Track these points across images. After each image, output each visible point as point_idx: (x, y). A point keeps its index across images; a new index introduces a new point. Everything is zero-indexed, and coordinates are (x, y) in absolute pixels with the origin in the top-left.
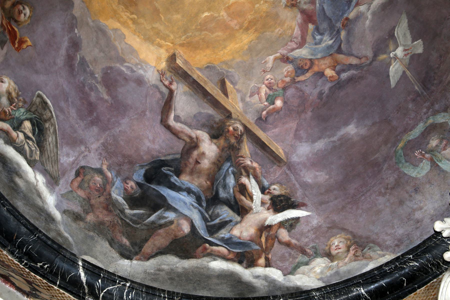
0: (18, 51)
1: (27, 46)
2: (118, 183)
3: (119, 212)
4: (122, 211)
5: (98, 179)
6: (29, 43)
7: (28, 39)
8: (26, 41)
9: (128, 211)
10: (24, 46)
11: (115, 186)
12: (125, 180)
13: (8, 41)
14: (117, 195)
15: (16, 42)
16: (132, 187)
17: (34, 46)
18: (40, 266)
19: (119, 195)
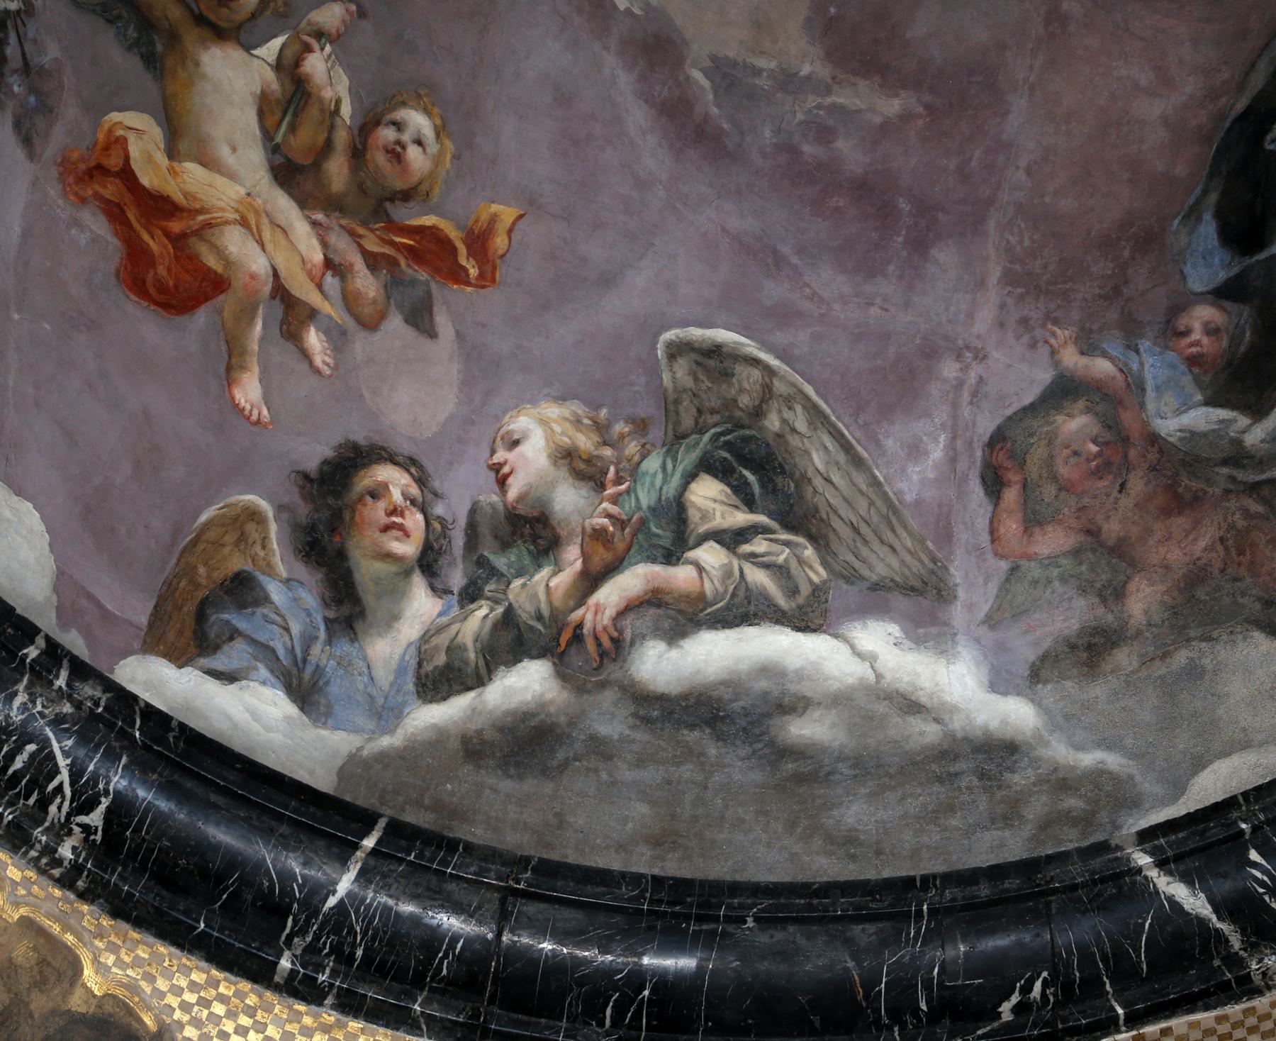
0: (493, 281)
1: (510, 232)
2: (1153, 364)
3: (1225, 470)
4: (1238, 456)
5: (1075, 424)
6: (507, 213)
7: (495, 208)
8: (494, 219)
9: (1256, 435)
10: (500, 242)
11: (1149, 386)
12: (1171, 332)
13: (433, 286)
14: (1179, 412)
15: (463, 261)
16: (1211, 331)
17: (531, 204)
18: (1016, 1010)
19: (1184, 408)
